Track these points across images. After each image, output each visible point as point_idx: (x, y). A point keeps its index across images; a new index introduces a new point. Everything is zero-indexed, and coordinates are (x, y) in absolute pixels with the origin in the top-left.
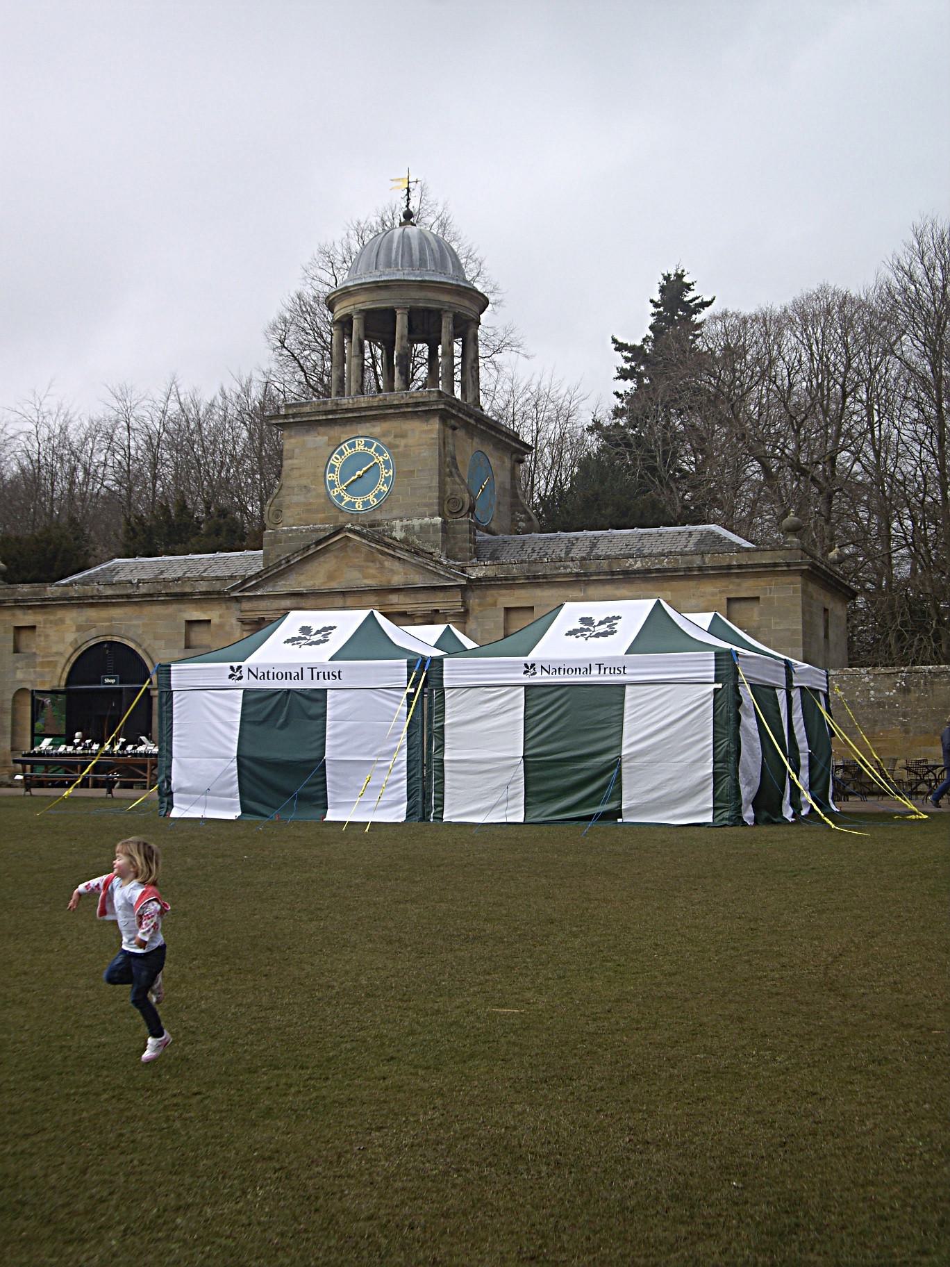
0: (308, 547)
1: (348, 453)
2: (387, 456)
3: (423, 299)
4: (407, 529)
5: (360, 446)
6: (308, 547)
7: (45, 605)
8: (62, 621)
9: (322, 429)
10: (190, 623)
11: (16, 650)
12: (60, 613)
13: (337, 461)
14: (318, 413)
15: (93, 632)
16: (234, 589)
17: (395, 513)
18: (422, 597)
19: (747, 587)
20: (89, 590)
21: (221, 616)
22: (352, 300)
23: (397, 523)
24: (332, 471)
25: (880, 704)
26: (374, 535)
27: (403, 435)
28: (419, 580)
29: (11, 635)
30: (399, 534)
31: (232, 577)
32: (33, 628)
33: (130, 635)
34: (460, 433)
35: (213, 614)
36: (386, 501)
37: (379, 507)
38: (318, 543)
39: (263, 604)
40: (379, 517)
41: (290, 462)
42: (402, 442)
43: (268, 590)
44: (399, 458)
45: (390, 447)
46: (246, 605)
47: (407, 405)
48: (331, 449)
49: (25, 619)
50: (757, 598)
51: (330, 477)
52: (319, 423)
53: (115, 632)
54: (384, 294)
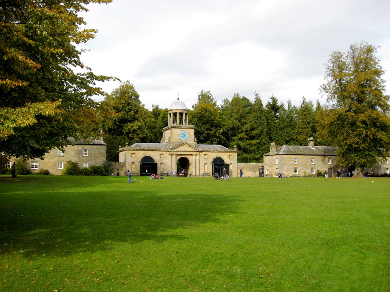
1: (182, 132)
10: (161, 154)
11: (131, 157)
12: (139, 151)
13: (180, 133)
15: (145, 154)
19: (231, 154)
20: (138, 148)
23: (189, 143)
27: (189, 131)
35: (164, 153)
40: (186, 141)
43: (173, 150)
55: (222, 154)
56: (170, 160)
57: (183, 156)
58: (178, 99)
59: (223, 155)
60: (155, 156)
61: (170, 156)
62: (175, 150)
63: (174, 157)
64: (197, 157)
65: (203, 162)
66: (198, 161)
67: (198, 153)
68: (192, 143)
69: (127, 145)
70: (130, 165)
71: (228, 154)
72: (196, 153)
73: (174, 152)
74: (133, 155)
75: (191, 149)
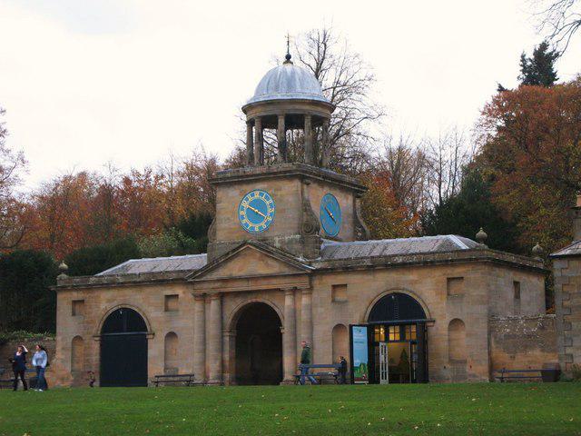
0: (228, 254)
2: (271, 201)
3: (292, 109)
4: (282, 242)
5: (257, 195)
6: (228, 254)
7: (90, 288)
8: (98, 297)
9: (236, 187)
13: (245, 204)
14: (235, 177)
15: (115, 303)
16: (189, 277)
17: (276, 233)
18: (287, 280)
21: (184, 293)
22: (254, 111)
23: (277, 239)
24: (242, 210)
25: (529, 336)
26: (263, 247)
28: (287, 271)
29: (70, 306)
30: (277, 245)
31: (189, 271)
32: (82, 301)
33: (136, 304)
34: (314, 186)
35: (179, 291)
36: (271, 225)
37: (267, 230)
38: (234, 250)
39: (206, 286)
40: (267, 235)
41: (222, 204)
42: (279, 193)
43: (208, 277)
44: (278, 200)
45: (273, 196)
46: (198, 286)
47: (280, 172)
48: (241, 198)
49: (76, 295)
50: (462, 278)
51: (242, 213)
52: (236, 183)
53: (127, 302)
54: (271, 107)
55: (411, 276)
56: (197, 317)
57: (254, 300)
58: (288, 57)
59: (416, 282)
60: (148, 304)
61: (197, 306)
62: (215, 275)
63: (214, 305)
64: (305, 300)
65: (327, 318)
66: (304, 316)
67: (302, 283)
68: (290, 242)
69: (63, 271)
70: (70, 345)
71: (439, 275)
72: (297, 283)
73: (212, 285)
74: (77, 307)
75: (275, 268)
